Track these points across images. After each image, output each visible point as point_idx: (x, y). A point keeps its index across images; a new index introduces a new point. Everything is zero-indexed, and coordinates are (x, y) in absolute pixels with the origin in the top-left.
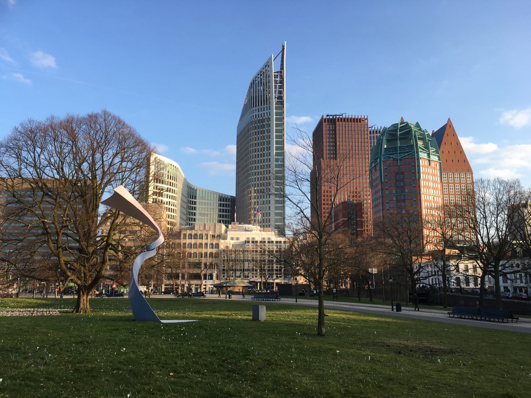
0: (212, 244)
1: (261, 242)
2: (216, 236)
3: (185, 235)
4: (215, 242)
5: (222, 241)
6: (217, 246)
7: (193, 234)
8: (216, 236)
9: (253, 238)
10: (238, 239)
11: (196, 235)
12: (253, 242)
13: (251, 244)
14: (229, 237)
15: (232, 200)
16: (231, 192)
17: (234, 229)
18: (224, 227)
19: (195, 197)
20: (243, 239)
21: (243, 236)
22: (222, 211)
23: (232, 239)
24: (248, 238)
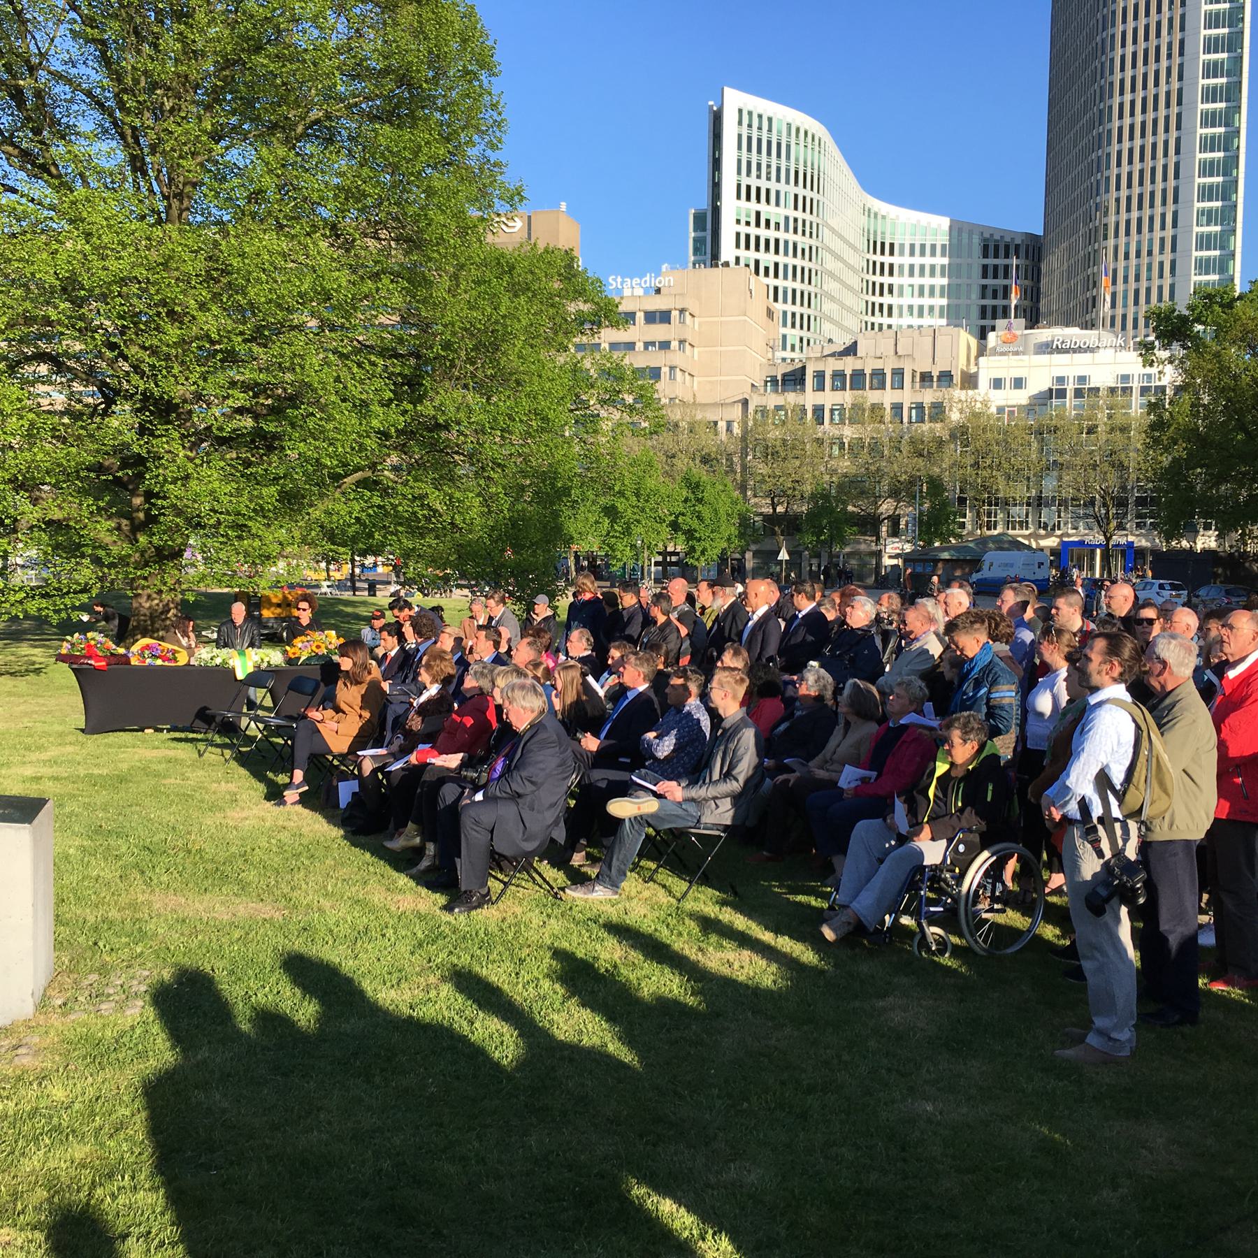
0: (920, 407)
1: (1112, 390)
2: (935, 374)
3: (820, 376)
4: (928, 397)
5: (958, 393)
6: (938, 411)
7: (848, 372)
8: (935, 374)
9: (1082, 379)
10: (1019, 383)
11: (858, 376)
12: (1078, 393)
13: (1070, 400)
14: (983, 382)
15: (1033, 250)
16: (1027, 217)
17: (1012, 348)
18: (966, 339)
19: (892, 245)
20: (1039, 382)
21: (1040, 373)
22: (989, 292)
23: (997, 384)
24: (1061, 380)
